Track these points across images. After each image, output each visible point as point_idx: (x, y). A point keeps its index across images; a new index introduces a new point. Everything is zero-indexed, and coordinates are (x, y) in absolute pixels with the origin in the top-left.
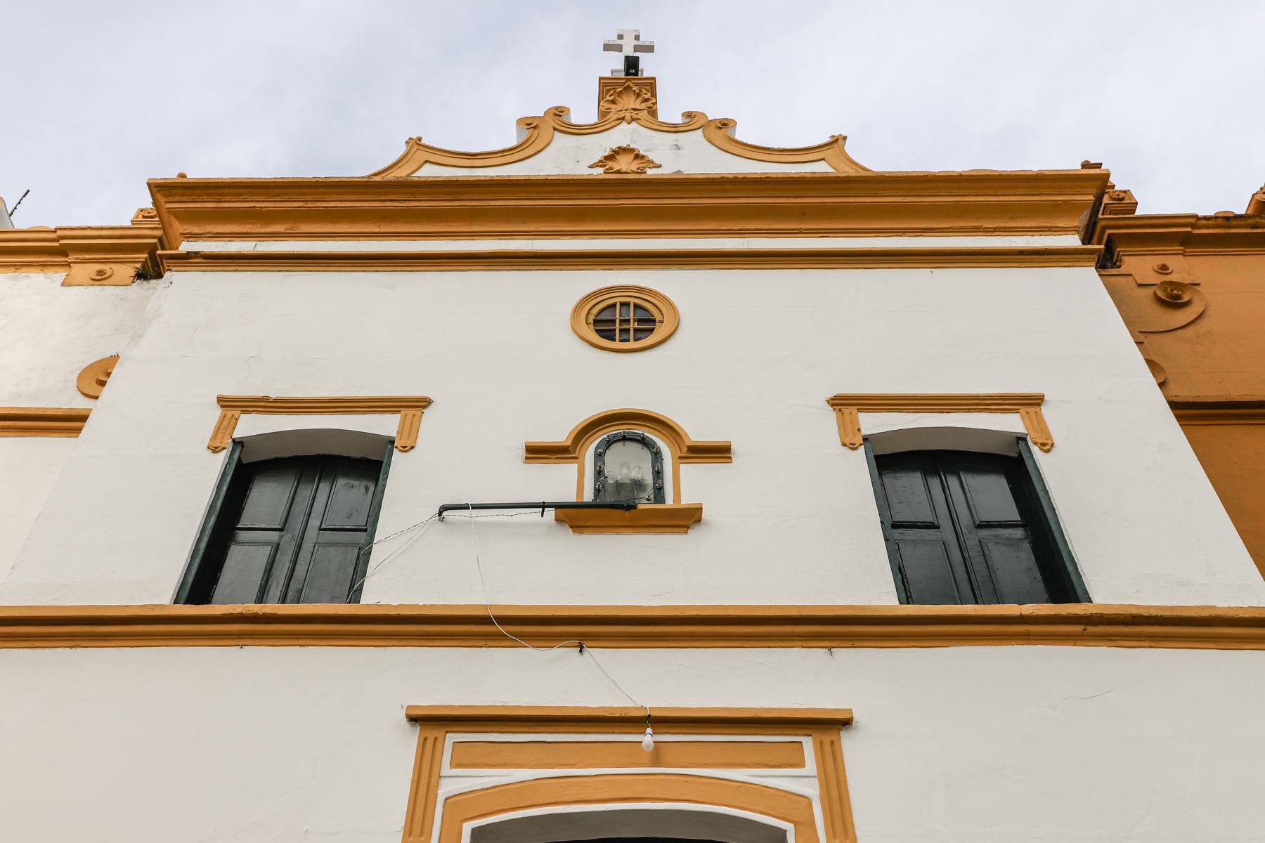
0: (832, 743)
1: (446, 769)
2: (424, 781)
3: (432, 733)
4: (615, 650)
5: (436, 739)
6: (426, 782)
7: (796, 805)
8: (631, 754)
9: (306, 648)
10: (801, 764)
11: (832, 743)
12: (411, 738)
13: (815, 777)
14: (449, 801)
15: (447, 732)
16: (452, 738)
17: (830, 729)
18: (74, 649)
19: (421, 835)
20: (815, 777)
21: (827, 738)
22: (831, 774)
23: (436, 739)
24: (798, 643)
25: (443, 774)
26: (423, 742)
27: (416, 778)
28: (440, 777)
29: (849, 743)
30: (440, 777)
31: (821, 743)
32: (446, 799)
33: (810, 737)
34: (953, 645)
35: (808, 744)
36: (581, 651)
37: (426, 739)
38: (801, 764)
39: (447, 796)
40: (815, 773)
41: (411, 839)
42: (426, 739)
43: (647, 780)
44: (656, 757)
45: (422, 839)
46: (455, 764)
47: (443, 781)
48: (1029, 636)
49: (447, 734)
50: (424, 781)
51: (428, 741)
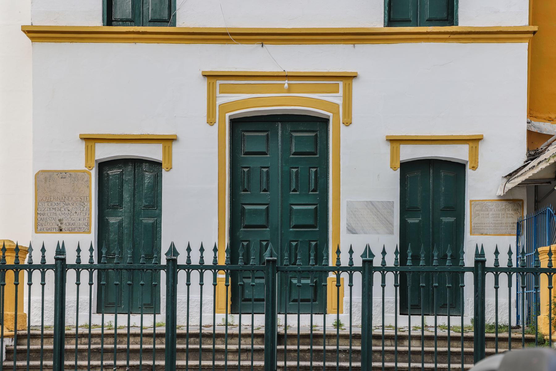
0: (349, 84)
1: (218, 94)
2: (211, 99)
3: (212, 80)
4: (275, 45)
5: (213, 83)
6: (212, 99)
7: (333, 107)
8: (280, 89)
9: (160, 44)
10: (338, 92)
11: (349, 84)
12: (204, 84)
13: (342, 96)
14: (220, 106)
15: (217, 80)
16: (219, 82)
17: (350, 79)
18: (72, 43)
19: (213, 118)
20: (342, 96)
21: (347, 82)
22: (347, 94)
23: (213, 83)
24: (343, 42)
25: (217, 96)
26: (209, 84)
27: (208, 98)
28: (216, 97)
29: (356, 85)
30: (216, 97)
31: (345, 84)
32: (219, 105)
33: (342, 82)
34: (399, 43)
35: (341, 84)
36: (262, 46)
37: (210, 83)
38: (338, 92)
39: (219, 104)
40: (342, 95)
41: (210, 119)
42: (210, 83)
43: (285, 99)
44: (289, 91)
45: (213, 119)
46: (221, 92)
47: (217, 98)
48: (429, 39)
49: (217, 81)
50: (211, 99)
51: (211, 84)
